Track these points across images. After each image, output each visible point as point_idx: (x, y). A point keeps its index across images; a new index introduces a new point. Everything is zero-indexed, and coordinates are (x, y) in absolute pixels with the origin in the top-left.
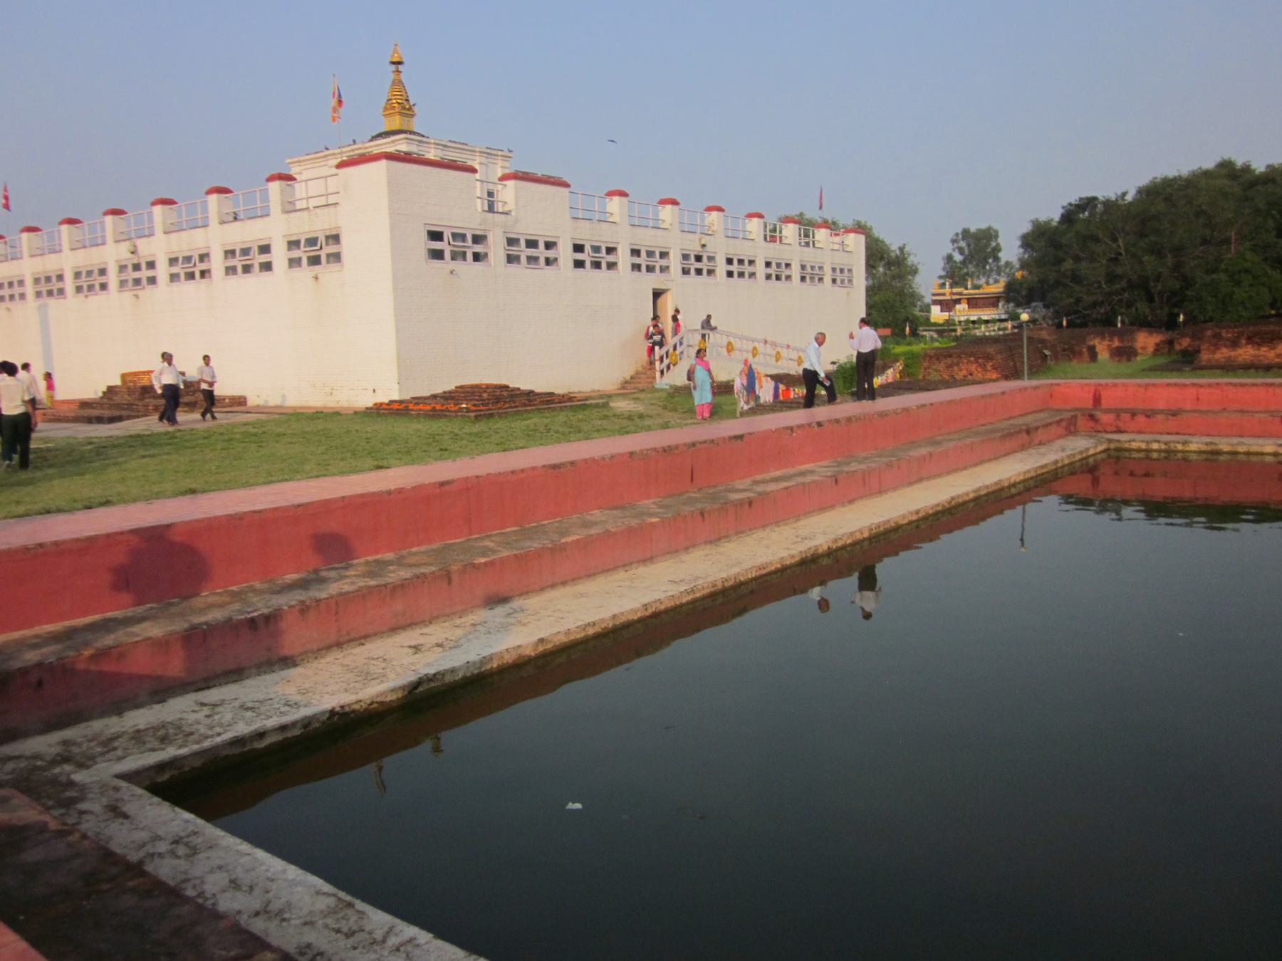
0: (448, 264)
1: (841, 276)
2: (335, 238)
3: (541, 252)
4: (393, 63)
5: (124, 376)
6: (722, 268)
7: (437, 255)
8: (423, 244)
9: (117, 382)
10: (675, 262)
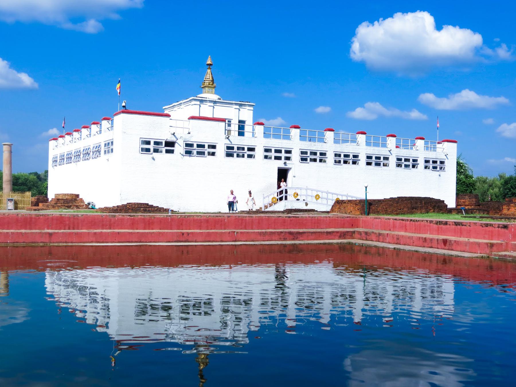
1: (436, 165)
2: (112, 143)
3: (207, 150)
4: (208, 65)
5: (55, 195)
6: (330, 158)
7: (148, 150)
8: (138, 146)
9: (54, 197)
10: (296, 156)
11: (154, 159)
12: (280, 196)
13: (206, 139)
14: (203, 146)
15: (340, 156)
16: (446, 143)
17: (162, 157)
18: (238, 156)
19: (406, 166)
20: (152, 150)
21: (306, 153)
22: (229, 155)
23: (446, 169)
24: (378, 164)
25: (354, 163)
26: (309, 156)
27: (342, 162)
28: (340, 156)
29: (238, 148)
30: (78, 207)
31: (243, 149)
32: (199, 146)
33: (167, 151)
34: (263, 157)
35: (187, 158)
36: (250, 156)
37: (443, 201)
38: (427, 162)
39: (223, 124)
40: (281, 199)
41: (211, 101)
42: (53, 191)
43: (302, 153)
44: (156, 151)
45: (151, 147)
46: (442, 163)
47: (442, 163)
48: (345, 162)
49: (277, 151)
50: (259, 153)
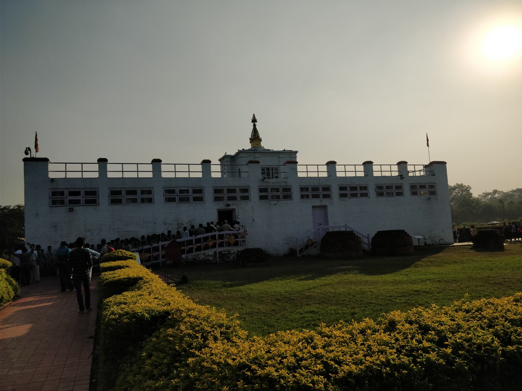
15: (307, 189)
16: (435, 165)
24: (354, 195)
26: (270, 194)
31: (188, 191)
36: (196, 199)
50: (209, 195)
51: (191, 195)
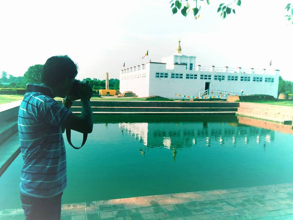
0: (160, 78)
3: (179, 76)
7: (158, 76)
8: (155, 75)
10: (213, 77)
11: (160, 79)
12: (206, 93)
13: (179, 73)
14: (178, 75)
15: (230, 77)
17: (163, 79)
18: (191, 78)
19: (258, 81)
20: (160, 76)
21: (217, 76)
22: (187, 78)
23: (274, 81)
24: (245, 80)
25: (236, 80)
27: (231, 79)
28: (230, 77)
29: (191, 75)
30: (133, 96)
31: (193, 75)
32: (176, 75)
33: (165, 77)
34: (200, 78)
35: (173, 79)
36: (195, 78)
37: (273, 96)
38: (266, 79)
39: (185, 66)
40: (207, 94)
41: (180, 56)
42: (123, 89)
43: (215, 76)
44: (161, 77)
45: (160, 75)
46: (273, 79)
47: (273, 79)
48: (232, 80)
49: (205, 76)
50: (199, 77)
51: (194, 77)
